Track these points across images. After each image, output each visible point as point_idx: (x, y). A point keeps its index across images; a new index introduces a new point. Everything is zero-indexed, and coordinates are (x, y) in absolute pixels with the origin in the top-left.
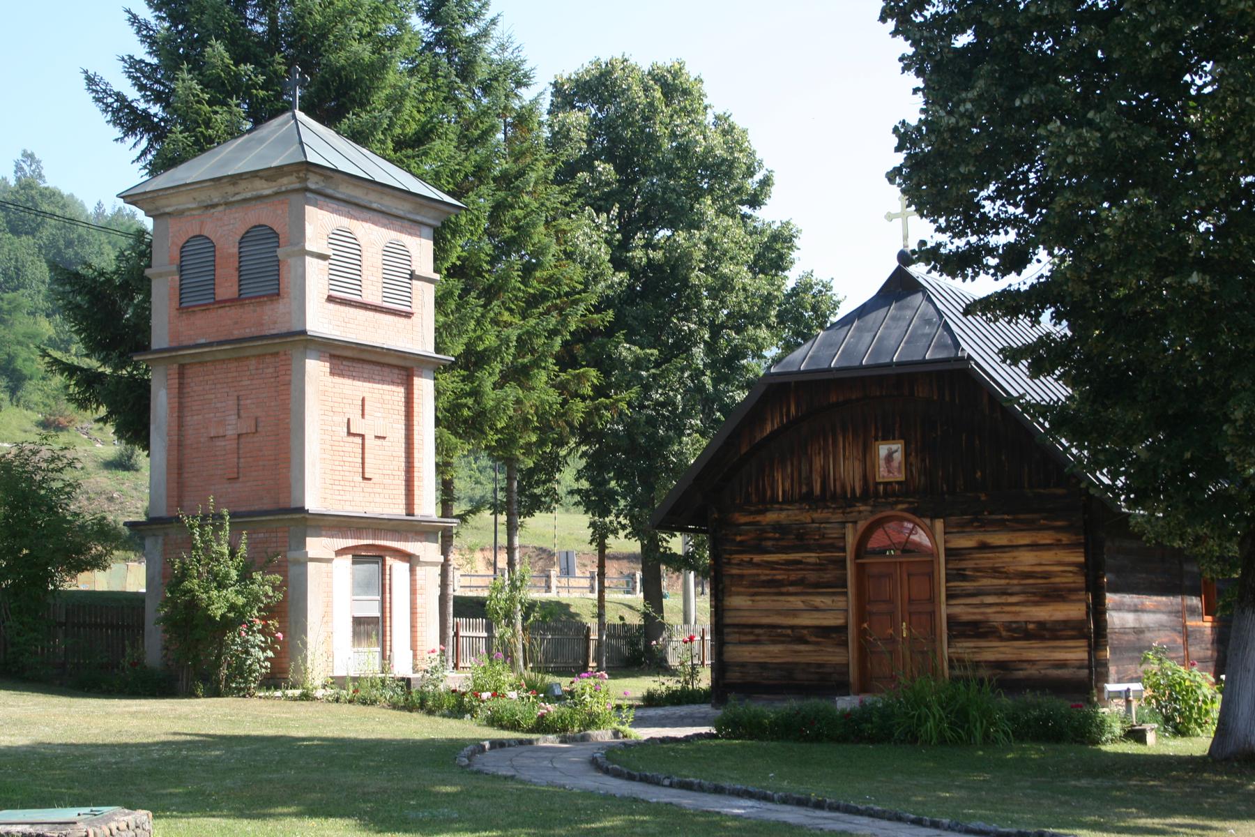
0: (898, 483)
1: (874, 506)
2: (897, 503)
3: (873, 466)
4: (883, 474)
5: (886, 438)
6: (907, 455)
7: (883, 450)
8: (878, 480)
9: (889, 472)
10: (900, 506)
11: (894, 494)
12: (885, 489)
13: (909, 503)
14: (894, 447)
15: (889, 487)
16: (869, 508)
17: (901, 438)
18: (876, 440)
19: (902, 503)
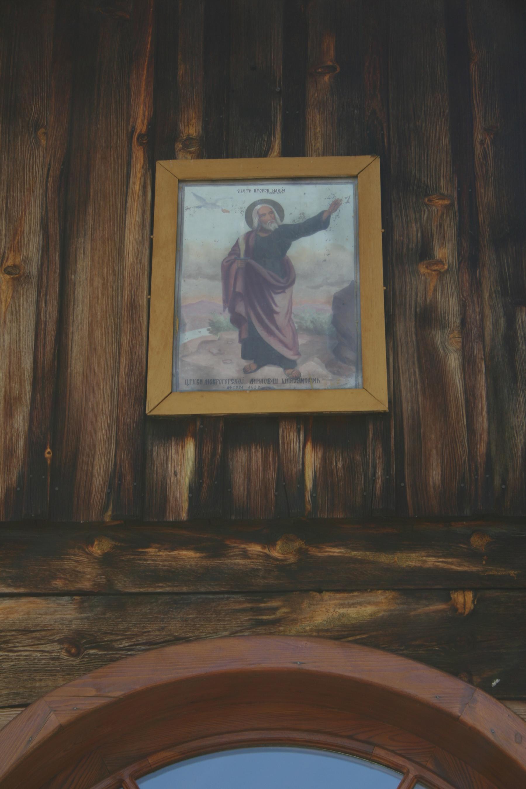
0: (320, 427)
1: (105, 597)
2: (305, 580)
3: (133, 319)
4: (201, 362)
5: (243, 130)
6: (399, 253)
7: (212, 215)
8: (161, 401)
9: (256, 352)
10: (329, 609)
11: (285, 514)
12: (212, 476)
13: (409, 585)
14: (300, 200)
15: (247, 464)
16: (63, 614)
17: (351, 139)
18: (160, 144)
19: (350, 581)
